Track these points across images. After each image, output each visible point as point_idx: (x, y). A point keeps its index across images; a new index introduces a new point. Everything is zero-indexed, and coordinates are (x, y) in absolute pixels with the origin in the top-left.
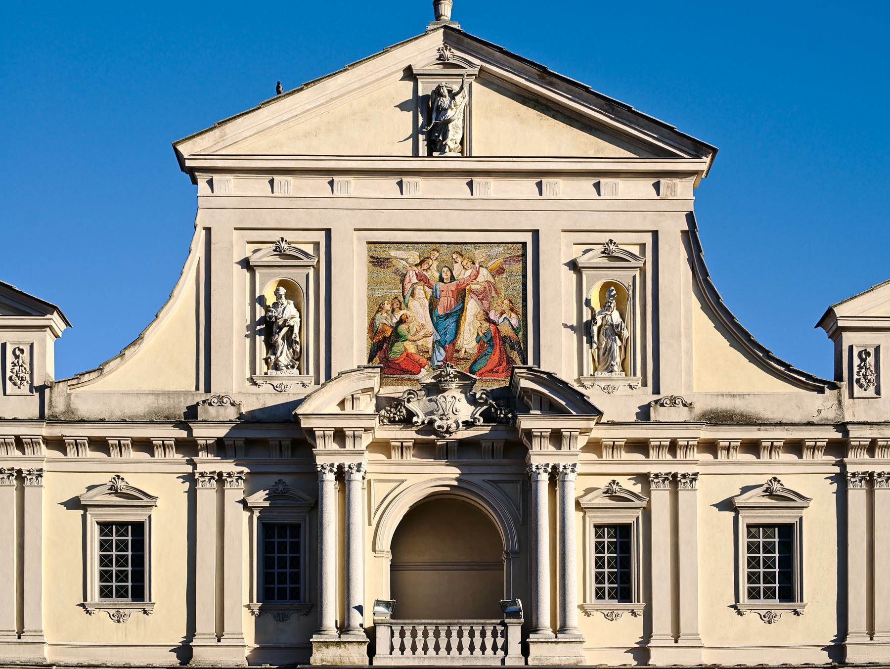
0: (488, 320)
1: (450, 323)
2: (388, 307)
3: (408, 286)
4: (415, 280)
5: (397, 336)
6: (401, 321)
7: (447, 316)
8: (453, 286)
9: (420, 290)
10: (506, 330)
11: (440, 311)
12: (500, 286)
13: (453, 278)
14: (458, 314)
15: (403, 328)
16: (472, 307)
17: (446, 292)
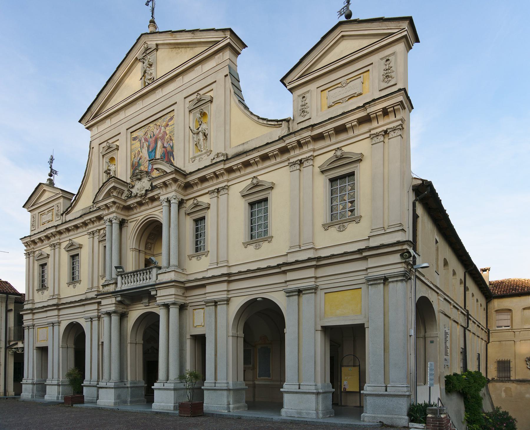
0: (164, 147)
1: (153, 154)
2: (137, 155)
3: (142, 144)
4: (144, 141)
5: (139, 165)
6: (140, 159)
7: (152, 151)
8: (154, 139)
9: (145, 145)
10: (169, 149)
11: (150, 150)
12: (168, 132)
13: (154, 135)
14: (155, 149)
15: (141, 160)
16: (159, 144)
17: (152, 140)
